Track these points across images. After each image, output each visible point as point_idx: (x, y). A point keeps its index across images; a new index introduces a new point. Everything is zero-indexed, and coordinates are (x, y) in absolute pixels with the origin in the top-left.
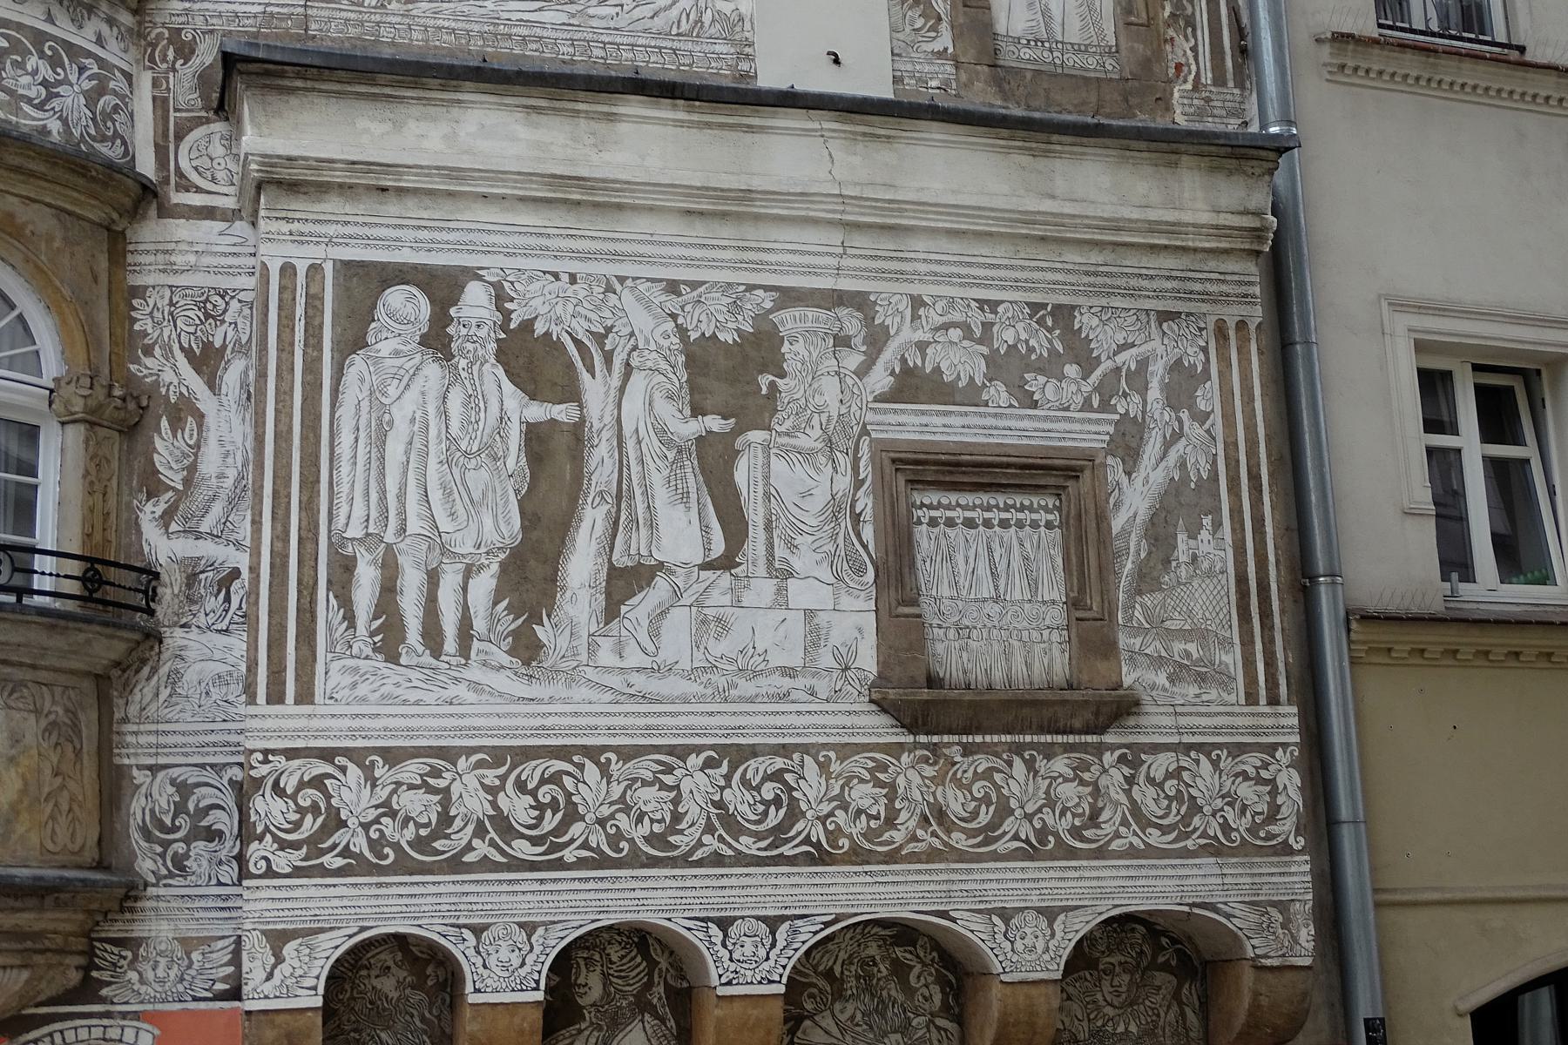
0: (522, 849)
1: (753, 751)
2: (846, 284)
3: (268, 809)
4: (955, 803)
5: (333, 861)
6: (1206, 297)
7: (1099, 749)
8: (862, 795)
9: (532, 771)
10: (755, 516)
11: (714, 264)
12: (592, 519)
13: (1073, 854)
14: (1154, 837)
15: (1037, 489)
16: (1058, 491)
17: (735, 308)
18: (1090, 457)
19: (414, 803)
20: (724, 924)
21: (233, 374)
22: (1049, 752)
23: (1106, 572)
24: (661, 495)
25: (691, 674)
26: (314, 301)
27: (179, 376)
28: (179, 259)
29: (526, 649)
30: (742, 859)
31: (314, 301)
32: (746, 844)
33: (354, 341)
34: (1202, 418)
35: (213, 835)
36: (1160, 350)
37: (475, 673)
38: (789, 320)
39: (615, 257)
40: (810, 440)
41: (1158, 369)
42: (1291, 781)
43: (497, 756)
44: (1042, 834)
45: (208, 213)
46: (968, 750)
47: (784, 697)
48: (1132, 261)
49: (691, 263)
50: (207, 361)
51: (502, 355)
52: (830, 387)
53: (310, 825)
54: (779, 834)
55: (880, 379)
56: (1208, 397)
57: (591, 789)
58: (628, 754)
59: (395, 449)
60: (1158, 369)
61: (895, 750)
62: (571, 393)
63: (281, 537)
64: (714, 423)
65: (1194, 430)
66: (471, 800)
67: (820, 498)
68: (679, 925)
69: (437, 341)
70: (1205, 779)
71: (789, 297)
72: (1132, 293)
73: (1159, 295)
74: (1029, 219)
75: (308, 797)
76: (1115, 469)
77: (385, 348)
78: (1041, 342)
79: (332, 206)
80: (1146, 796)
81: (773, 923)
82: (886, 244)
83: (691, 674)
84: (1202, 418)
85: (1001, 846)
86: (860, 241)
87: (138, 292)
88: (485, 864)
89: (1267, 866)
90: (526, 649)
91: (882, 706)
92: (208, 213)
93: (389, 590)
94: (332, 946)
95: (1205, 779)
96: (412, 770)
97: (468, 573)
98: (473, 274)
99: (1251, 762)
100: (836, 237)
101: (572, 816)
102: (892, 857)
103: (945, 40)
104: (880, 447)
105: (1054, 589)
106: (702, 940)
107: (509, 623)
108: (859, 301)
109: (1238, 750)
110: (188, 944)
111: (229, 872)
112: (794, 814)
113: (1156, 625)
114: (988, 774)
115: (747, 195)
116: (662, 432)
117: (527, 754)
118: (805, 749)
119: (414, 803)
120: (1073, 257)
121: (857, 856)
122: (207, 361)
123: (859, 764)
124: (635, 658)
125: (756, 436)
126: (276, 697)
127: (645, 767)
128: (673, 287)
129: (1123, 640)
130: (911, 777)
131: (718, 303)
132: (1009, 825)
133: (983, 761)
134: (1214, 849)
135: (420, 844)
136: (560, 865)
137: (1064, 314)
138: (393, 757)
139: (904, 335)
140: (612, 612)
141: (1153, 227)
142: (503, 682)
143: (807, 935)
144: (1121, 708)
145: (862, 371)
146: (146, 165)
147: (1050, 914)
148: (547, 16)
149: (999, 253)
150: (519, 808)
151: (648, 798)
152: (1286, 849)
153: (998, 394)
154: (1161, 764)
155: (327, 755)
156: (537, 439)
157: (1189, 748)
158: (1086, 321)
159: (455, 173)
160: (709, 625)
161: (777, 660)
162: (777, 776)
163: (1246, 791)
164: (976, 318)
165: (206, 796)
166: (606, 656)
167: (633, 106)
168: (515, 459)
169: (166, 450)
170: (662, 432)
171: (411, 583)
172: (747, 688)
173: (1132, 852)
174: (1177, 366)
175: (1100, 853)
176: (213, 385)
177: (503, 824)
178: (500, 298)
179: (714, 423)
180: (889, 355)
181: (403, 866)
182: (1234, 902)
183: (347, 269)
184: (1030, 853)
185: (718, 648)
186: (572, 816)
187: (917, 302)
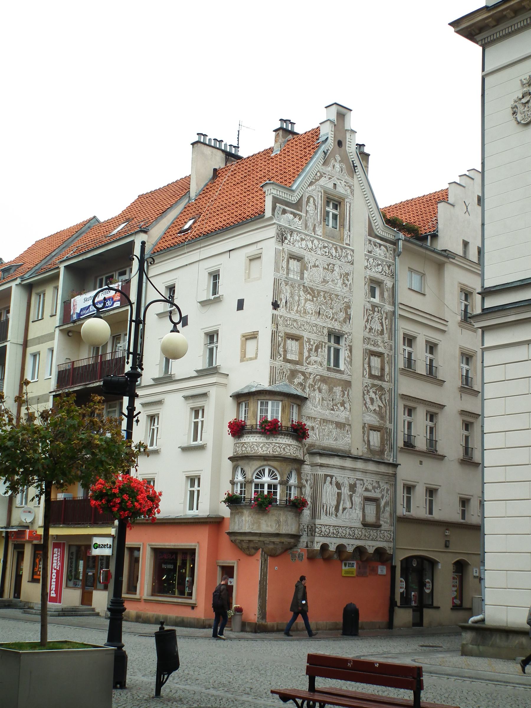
0: (335, 536)
1: (352, 528)
2: (362, 478)
3: (317, 530)
4: (367, 534)
5: (321, 535)
6: (390, 481)
7: (378, 530)
8: (360, 533)
9: (336, 528)
10: (354, 503)
11: (351, 475)
12: (342, 502)
13: (375, 540)
14: (381, 540)
15: (375, 501)
16: (376, 502)
17: (353, 480)
18: (379, 498)
19: (327, 530)
20: (349, 545)
21: (309, 482)
22: (374, 530)
23: (380, 511)
24: (347, 500)
25: (348, 519)
26: (322, 478)
27: (304, 482)
28: (305, 470)
29: (336, 516)
30: (351, 538)
31: (322, 478)
32: (351, 537)
33: (325, 483)
34: (389, 494)
35: (305, 531)
36: (386, 486)
37: (332, 518)
38: (358, 482)
39: (344, 474)
40: (358, 495)
41: (385, 489)
42: (392, 534)
43: (334, 526)
44: (373, 538)
45: (307, 465)
46: (368, 529)
47: (355, 522)
48: (385, 477)
49: (350, 475)
50: (307, 481)
51: (336, 485)
52: (360, 489)
53: (320, 532)
54: (353, 536)
55: (364, 489)
56: (389, 492)
57: (340, 530)
58: (343, 527)
59: (327, 494)
60: (385, 489)
61: (363, 528)
62: (340, 489)
63: (319, 503)
64: (351, 493)
65: (388, 496)
66: (332, 531)
67: (358, 502)
68: (346, 544)
69: (331, 483)
70: (386, 534)
71: (357, 479)
72: (384, 480)
73: (386, 480)
74: (377, 472)
75: (320, 529)
76: (381, 500)
77: (327, 483)
78: (377, 485)
79: (324, 468)
80: (381, 535)
81: (352, 545)
82: (365, 474)
83: (348, 519)
84: (389, 494)
85: (370, 539)
86: (363, 473)
87: (302, 473)
88: (332, 537)
89: (390, 543)
90: (336, 516)
91: (362, 524)
92: (307, 465)
93: (327, 509)
94: (321, 544)
95: (386, 534)
96: (328, 527)
97: (333, 507)
98: (333, 476)
99: (390, 532)
100: (361, 473)
101: (339, 533)
102: (362, 539)
103: (366, 446)
104: (364, 496)
105: (375, 512)
106: (347, 546)
107: (335, 513)
108: (362, 480)
109: (388, 531)
110: (303, 542)
111: (306, 535)
112: (355, 534)
113: (383, 517)
114: (369, 532)
115: (355, 468)
116: (347, 494)
117: (336, 526)
118: (356, 528)
119: (327, 530)
120: (380, 476)
121: (359, 539)
122: (307, 481)
123: (360, 530)
124: (344, 517)
125: (354, 494)
126: (318, 519)
127: (344, 528)
128: (349, 478)
129: (381, 519)
130: (363, 531)
131: (352, 479)
132: (371, 537)
133: (369, 530)
134: (386, 541)
135: (328, 534)
136: (337, 538)
137: (379, 482)
138: (326, 525)
139: (366, 484)
140: (343, 513)
141: (387, 473)
142: (334, 519)
143: (355, 546)
144: (380, 526)
145: (362, 488)
146: (302, 459)
147: (373, 546)
148: (334, 443)
149: (373, 475)
150: (335, 531)
151: (344, 531)
152: (391, 542)
153: (373, 491)
154: (382, 532)
155: (321, 525)
156: (338, 493)
157: (384, 530)
158: (380, 483)
159: (334, 465)
160: (350, 514)
161: (355, 518)
162: (354, 530)
163: (389, 535)
164: (372, 482)
165: (305, 527)
166: (342, 517)
167: (348, 459)
168: (336, 496)
169: (303, 490)
170: (347, 494)
171: (328, 508)
172: (352, 521)
173: (379, 541)
174: (387, 489)
175: (377, 541)
176: (307, 483)
177: (333, 533)
178: (336, 478)
179: (351, 493)
180: (364, 487)
181: (326, 537)
182: (387, 547)
183: (325, 475)
184: (372, 540)
185: (351, 517)
186: (339, 533)
187: (367, 480)
